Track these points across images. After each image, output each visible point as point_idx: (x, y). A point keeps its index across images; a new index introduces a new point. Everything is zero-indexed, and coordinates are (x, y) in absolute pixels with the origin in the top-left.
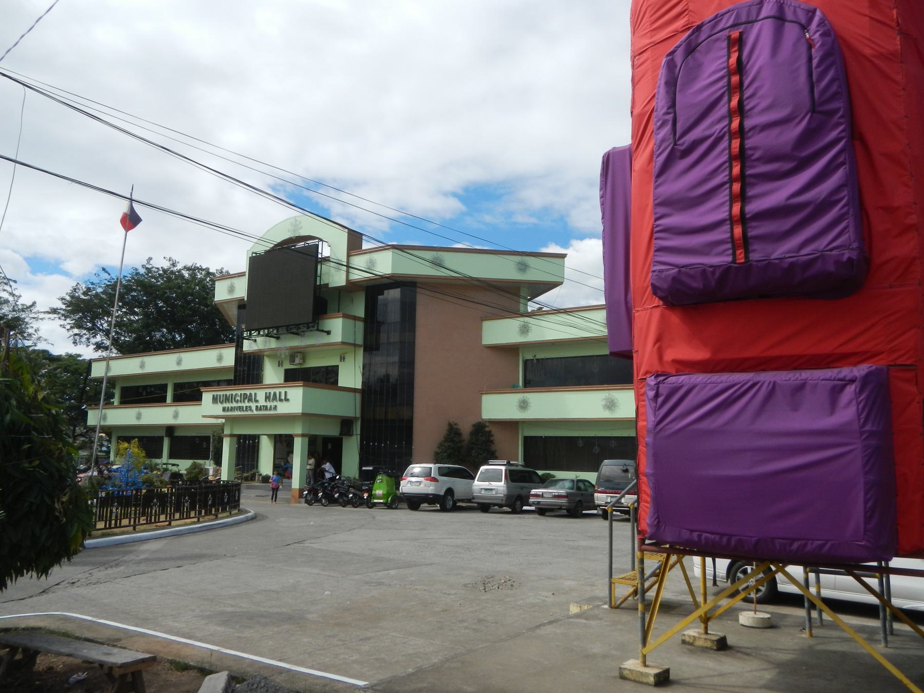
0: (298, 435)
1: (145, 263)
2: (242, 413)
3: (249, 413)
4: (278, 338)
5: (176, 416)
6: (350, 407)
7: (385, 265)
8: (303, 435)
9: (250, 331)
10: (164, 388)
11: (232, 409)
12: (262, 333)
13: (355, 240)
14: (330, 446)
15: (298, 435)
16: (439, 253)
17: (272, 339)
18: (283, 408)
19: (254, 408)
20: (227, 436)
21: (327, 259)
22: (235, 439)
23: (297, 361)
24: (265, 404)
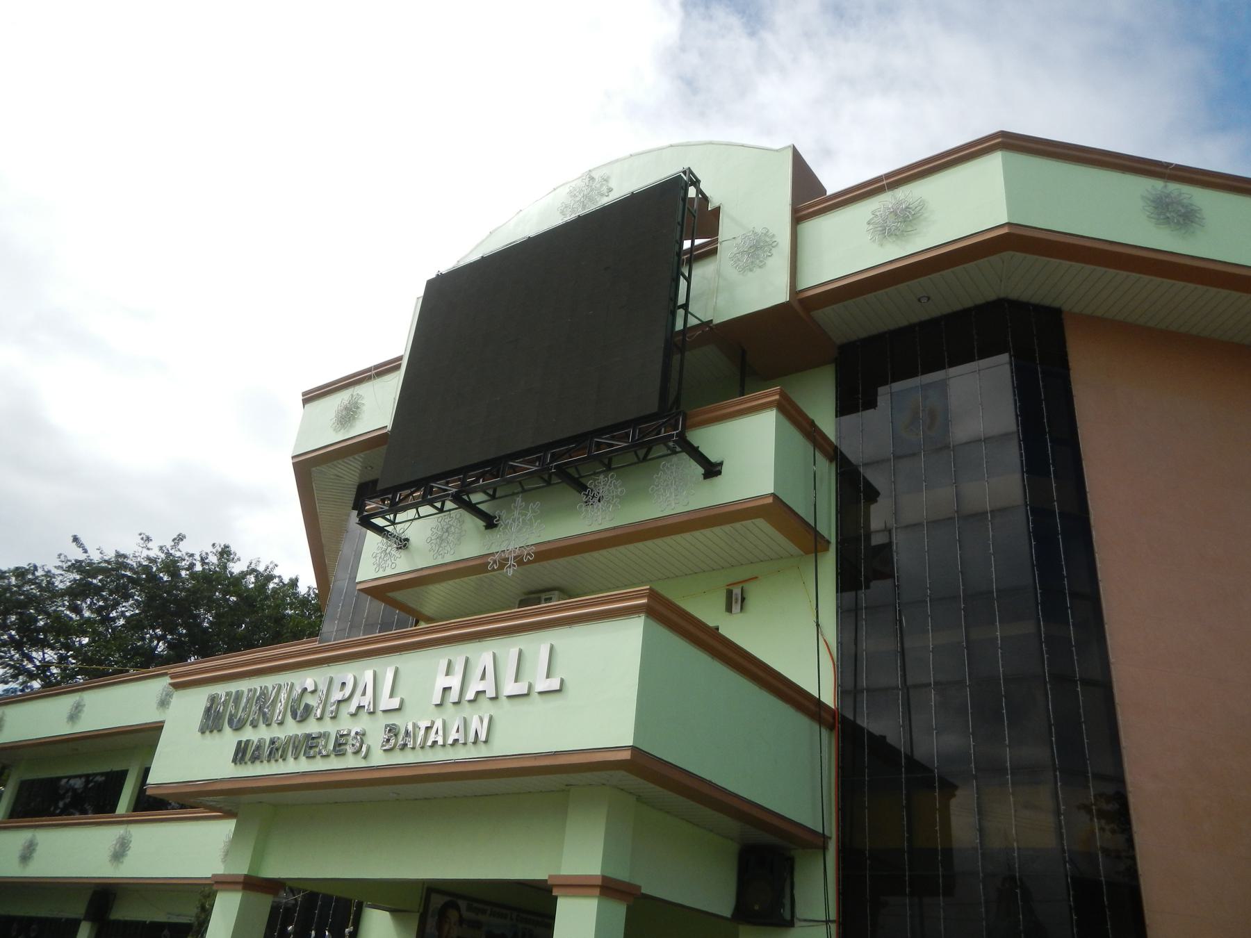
0: (578, 886)
1: (169, 544)
2: (319, 765)
3: (350, 761)
4: (490, 523)
5: (119, 854)
6: (790, 780)
7: (969, 207)
8: (608, 888)
11: (276, 750)
13: (809, 200)
15: (578, 886)
16: (1174, 188)
17: (472, 523)
18: (525, 734)
19: (376, 738)
22: (264, 903)
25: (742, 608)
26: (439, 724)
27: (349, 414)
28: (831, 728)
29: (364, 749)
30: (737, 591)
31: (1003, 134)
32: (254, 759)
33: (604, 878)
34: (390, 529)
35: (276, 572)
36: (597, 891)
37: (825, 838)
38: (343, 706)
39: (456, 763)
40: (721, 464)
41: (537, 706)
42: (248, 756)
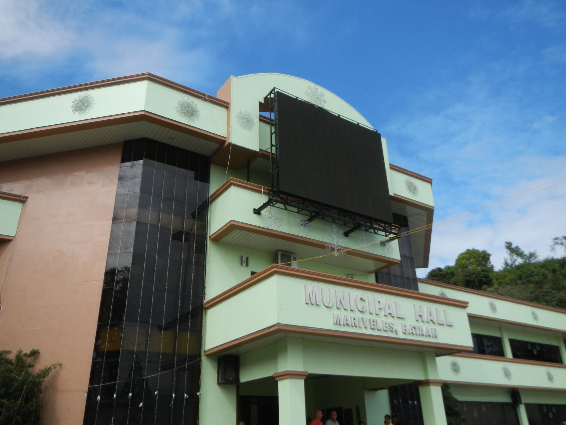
15: (436, 383)
24: (415, 324)
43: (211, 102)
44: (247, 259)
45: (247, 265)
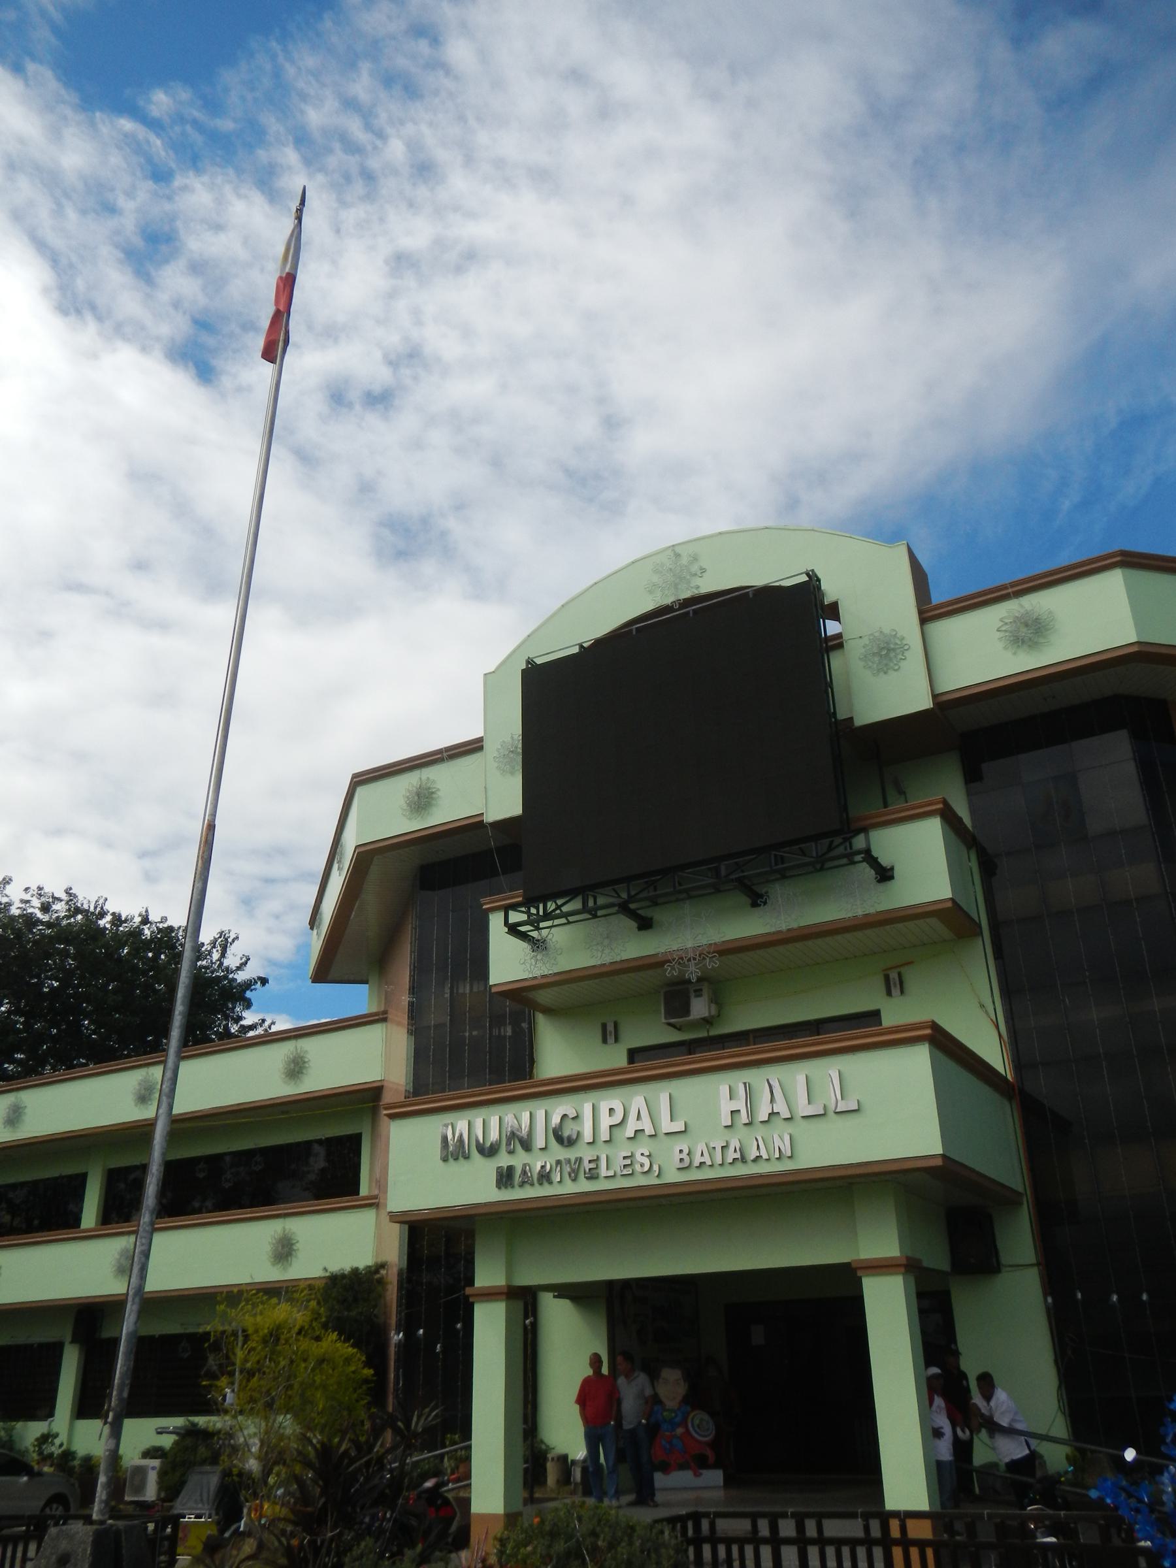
0: (881, 1267)
9: (544, 899)
10: (77, 1185)
12: (591, 903)
14: (758, 1335)
15: (881, 1267)
20: (490, 1295)
21: (837, 643)
23: (700, 1008)
25: (902, 992)
26: (734, 1143)
27: (422, 800)
28: (1010, 1099)
29: (656, 1168)
30: (894, 975)
31: (1123, 553)
32: (522, 1185)
33: (908, 1258)
34: (535, 934)
35: (111, 907)
36: (903, 1270)
37: (1019, 1194)
38: (614, 1129)
39: (761, 1176)
40: (892, 869)
41: (835, 1125)
42: (517, 1178)
43: (452, 757)
44: (616, 1025)
45: (616, 1040)
